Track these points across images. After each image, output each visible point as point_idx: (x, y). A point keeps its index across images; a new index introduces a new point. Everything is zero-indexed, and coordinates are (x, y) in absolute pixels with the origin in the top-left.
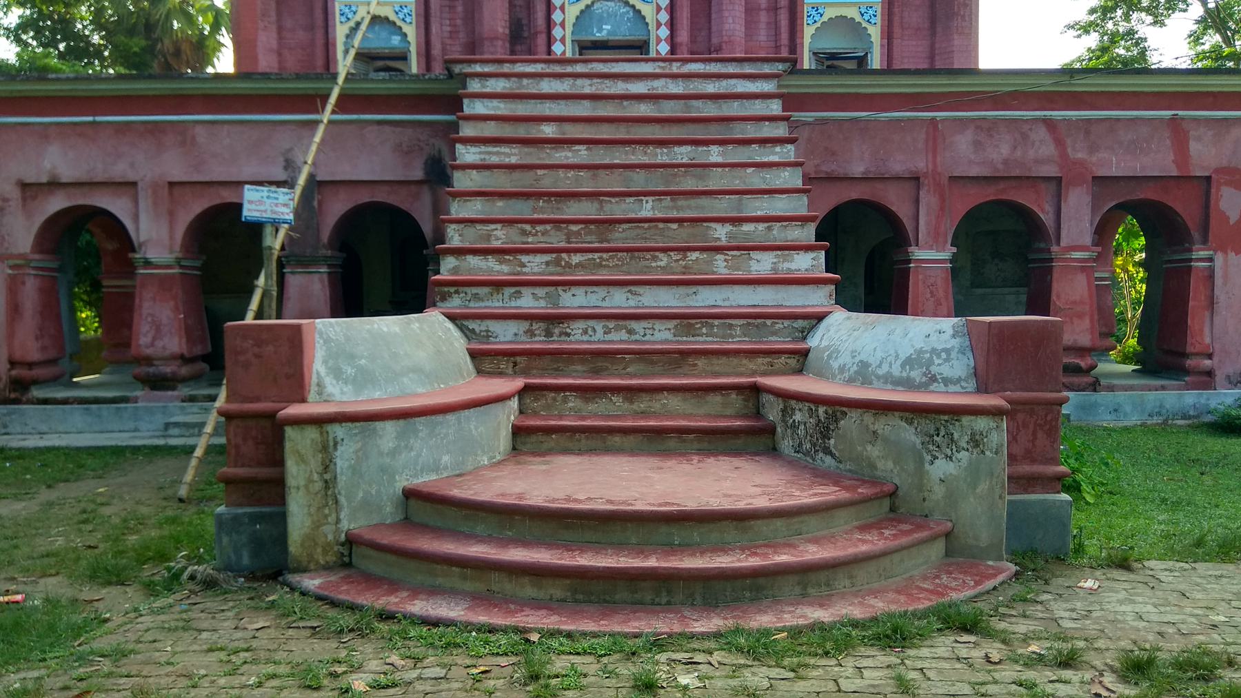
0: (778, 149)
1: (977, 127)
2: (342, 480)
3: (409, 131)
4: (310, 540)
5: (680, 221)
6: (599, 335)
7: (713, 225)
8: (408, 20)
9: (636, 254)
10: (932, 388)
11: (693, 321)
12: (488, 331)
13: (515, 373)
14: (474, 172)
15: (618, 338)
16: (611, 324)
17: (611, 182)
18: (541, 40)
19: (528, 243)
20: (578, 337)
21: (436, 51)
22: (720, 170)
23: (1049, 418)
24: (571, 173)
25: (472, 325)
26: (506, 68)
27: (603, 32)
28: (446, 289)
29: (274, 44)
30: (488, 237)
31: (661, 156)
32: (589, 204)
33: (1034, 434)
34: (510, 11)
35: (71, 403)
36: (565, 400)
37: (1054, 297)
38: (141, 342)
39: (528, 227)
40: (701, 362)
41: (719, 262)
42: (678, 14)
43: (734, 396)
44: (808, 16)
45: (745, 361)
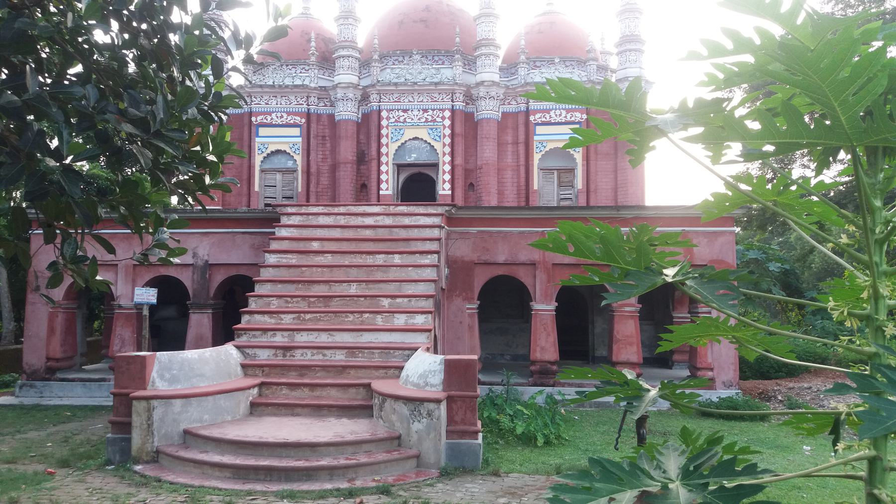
0: (429, 256)
2: (155, 425)
3: (259, 238)
4: (141, 449)
5: (365, 297)
6: (309, 357)
7: (382, 299)
8: (297, 152)
9: (338, 314)
10: (426, 388)
11: (355, 350)
12: (255, 354)
13: (263, 376)
14: (271, 269)
15: (316, 358)
16: (315, 351)
18: (374, 164)
19: (288, 307)
20: (298, 358)
21: (313, 169)
22: (395, 268)
23: (472, 404)
24: (320, 269)
25: (248, 351)
26: (303, 210)
27: (412, 158)
28: (240, 332)
30: (269, 304)
31: (369, 260)
32: (324, 286)
33: (465, 412)
34: (357, 146)
35: (77, 381)
36: (281, 390)
37: (615, 333)
38: (114, 349)
39: (289, 299)
40: (352, 372)
41: (379, 319)
42: (456, 148)
43: (361, 389)
44: (537, 148)
45: (374, 372)
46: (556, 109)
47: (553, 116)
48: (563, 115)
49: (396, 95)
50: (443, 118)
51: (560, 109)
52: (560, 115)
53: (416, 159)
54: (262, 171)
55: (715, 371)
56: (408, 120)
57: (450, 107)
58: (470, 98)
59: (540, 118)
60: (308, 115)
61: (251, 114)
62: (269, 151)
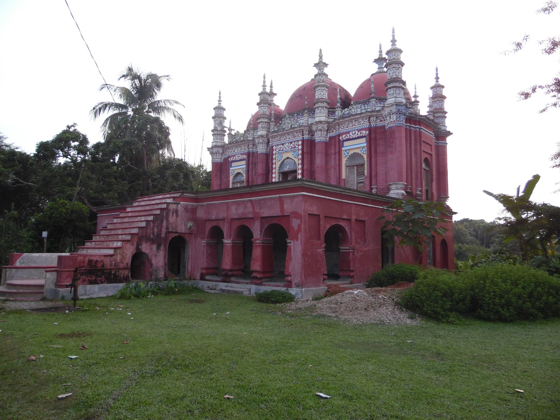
1: (236, 204)
17: (127, 225)
24: (119, 224)
29: (219, 183)
37: (252, 255)
46: (352, 131)
47: (352, 135)
48: (356, 134)
49: (279, 137)
50: (298, 145)
51: (354, 131)
52: (355, 134)
53: (289, 169)
54: (233, 183)
55: (292, 277)
56: (284, 149)
57: (301, 139)
58: (311, 133)
59: (345, 137)
60: (248, 154)
61: (229, 157)
62: (235, 174)
